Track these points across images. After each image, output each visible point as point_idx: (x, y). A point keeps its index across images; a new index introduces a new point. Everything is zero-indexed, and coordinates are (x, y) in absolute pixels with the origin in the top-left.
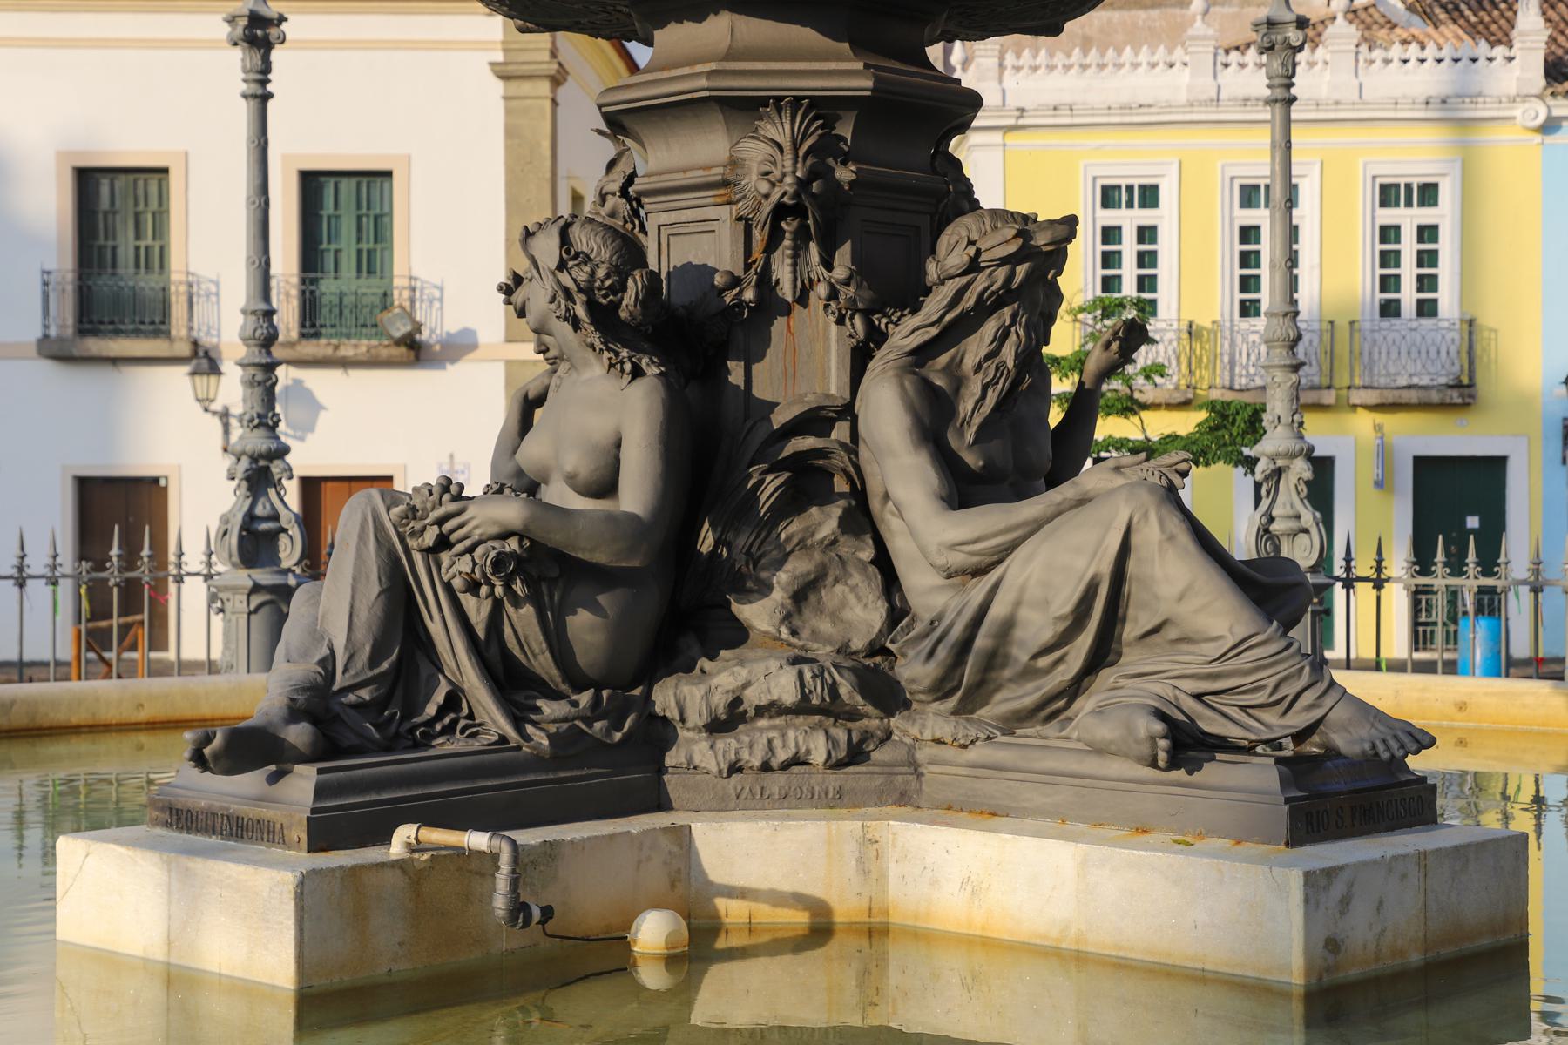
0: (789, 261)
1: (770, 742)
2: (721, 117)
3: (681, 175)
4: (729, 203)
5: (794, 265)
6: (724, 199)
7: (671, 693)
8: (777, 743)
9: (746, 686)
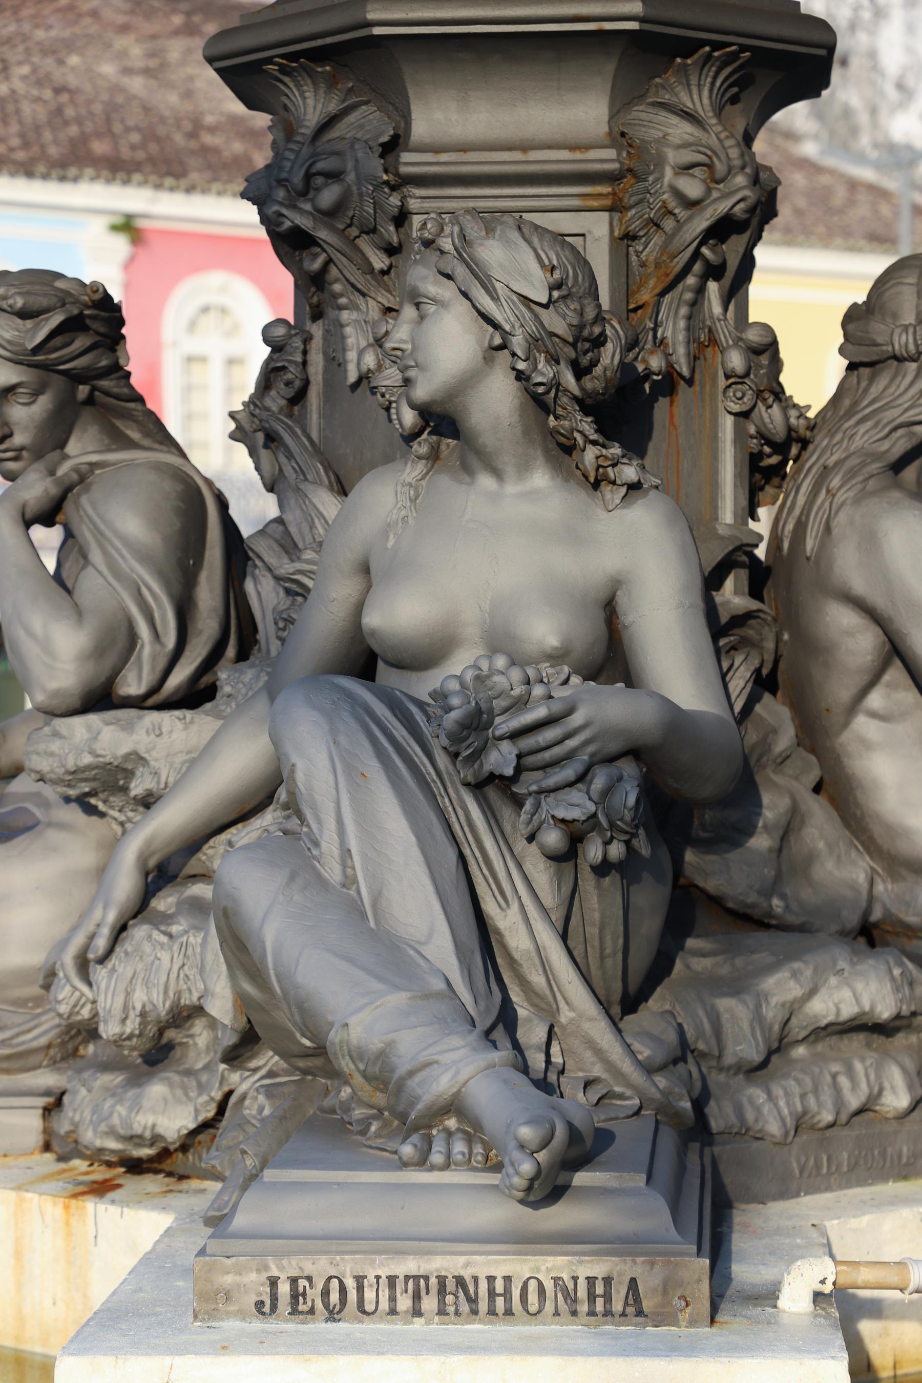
0: (684, 311)
1: (834, 1076)
2: (610, 67)
3: (517, 156)
4: (610, 209)
5: (689, 318)
6: (608, 202)
7: (701, 1013)
8: (843, 1081)
9: (812, 993)
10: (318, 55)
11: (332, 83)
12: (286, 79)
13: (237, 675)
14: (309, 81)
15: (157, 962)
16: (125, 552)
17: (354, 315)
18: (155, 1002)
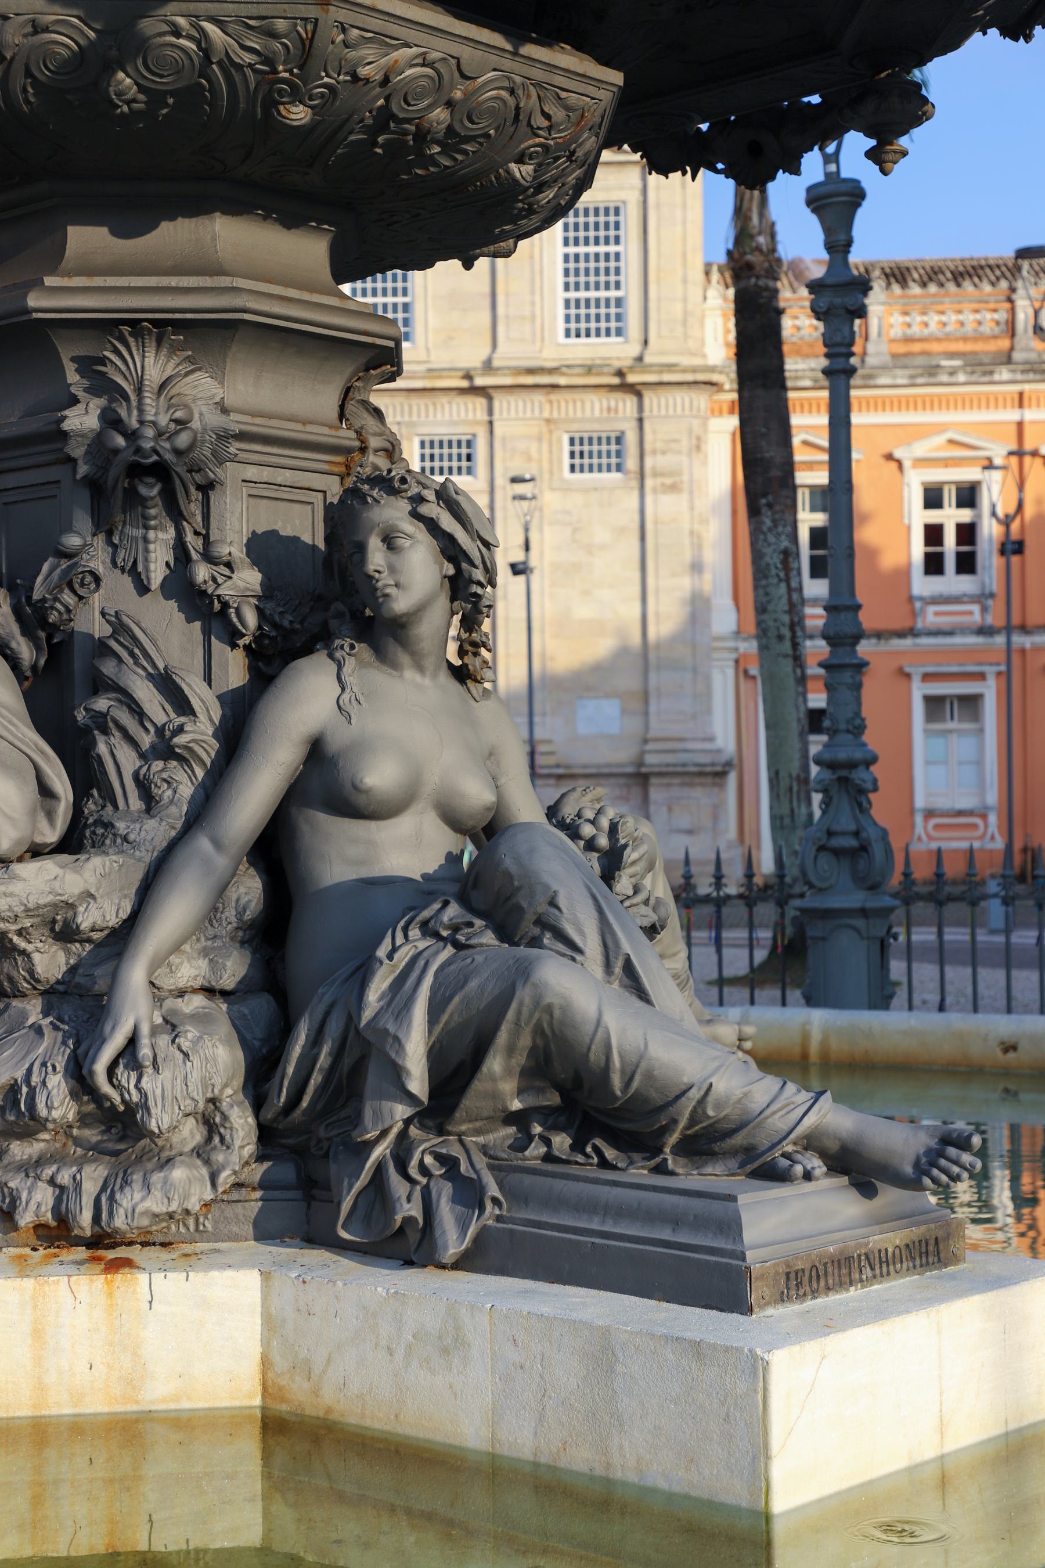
10: (179, 326)
11: (174, 349)
12: (131, 341)
13: (138, 826)
14: (154, 344)
15: (189, 1064)
16: (15, 721)
17: (161, 535)
18: (196, 1098)
